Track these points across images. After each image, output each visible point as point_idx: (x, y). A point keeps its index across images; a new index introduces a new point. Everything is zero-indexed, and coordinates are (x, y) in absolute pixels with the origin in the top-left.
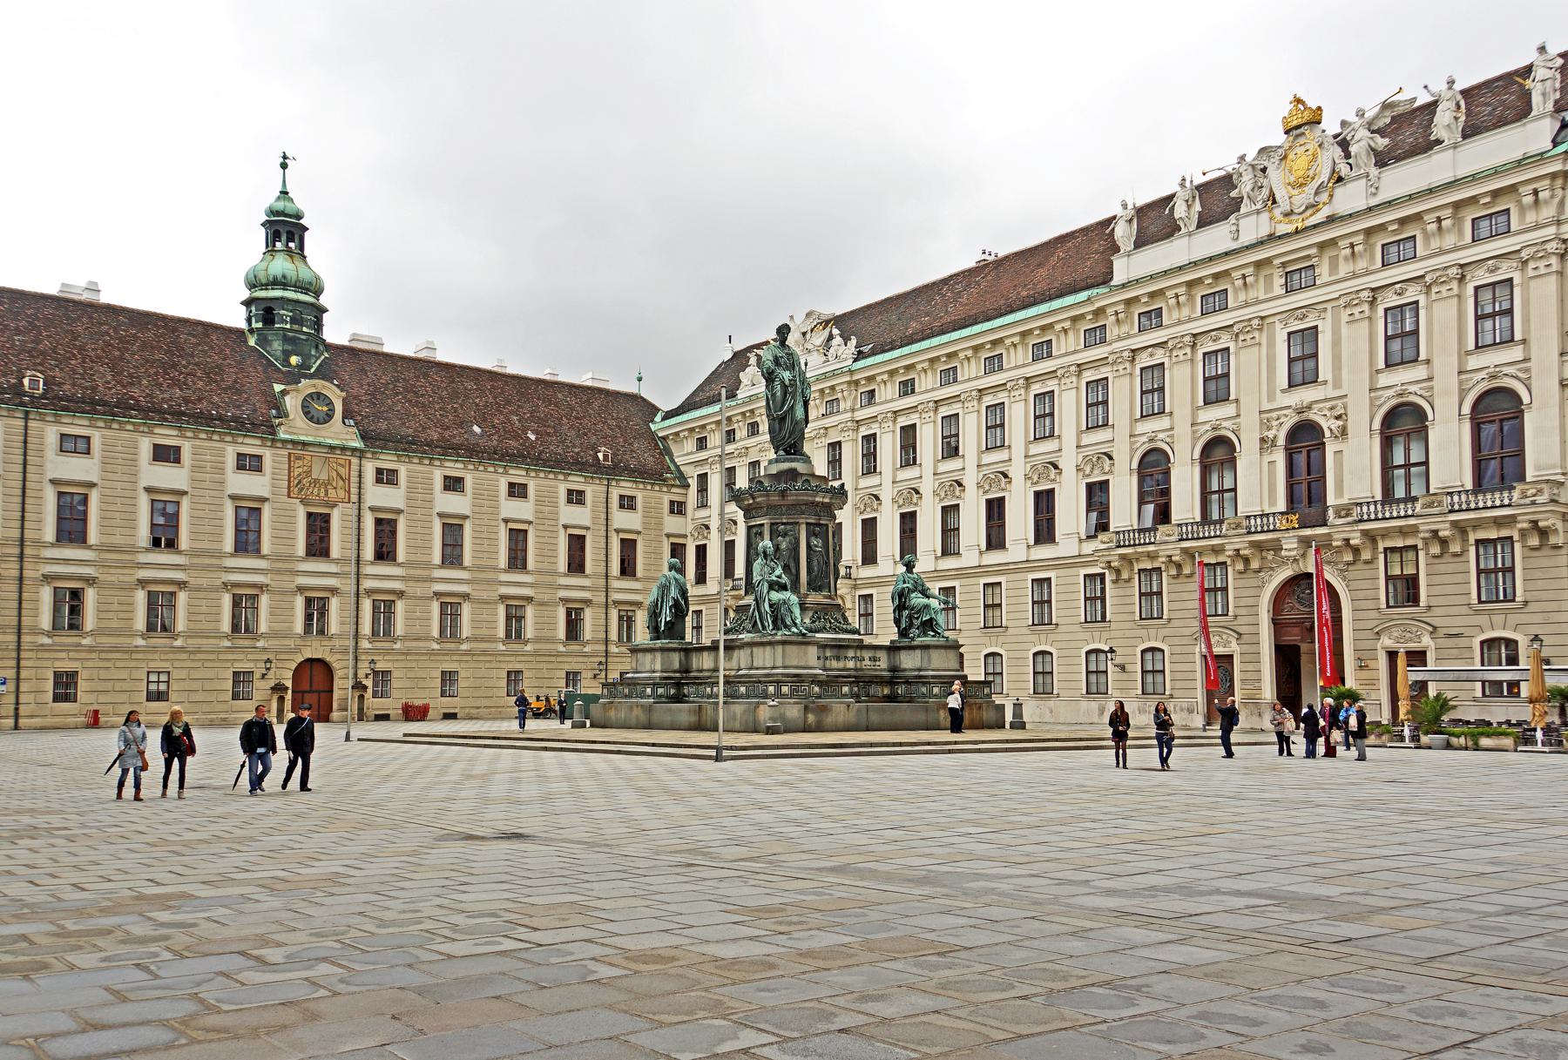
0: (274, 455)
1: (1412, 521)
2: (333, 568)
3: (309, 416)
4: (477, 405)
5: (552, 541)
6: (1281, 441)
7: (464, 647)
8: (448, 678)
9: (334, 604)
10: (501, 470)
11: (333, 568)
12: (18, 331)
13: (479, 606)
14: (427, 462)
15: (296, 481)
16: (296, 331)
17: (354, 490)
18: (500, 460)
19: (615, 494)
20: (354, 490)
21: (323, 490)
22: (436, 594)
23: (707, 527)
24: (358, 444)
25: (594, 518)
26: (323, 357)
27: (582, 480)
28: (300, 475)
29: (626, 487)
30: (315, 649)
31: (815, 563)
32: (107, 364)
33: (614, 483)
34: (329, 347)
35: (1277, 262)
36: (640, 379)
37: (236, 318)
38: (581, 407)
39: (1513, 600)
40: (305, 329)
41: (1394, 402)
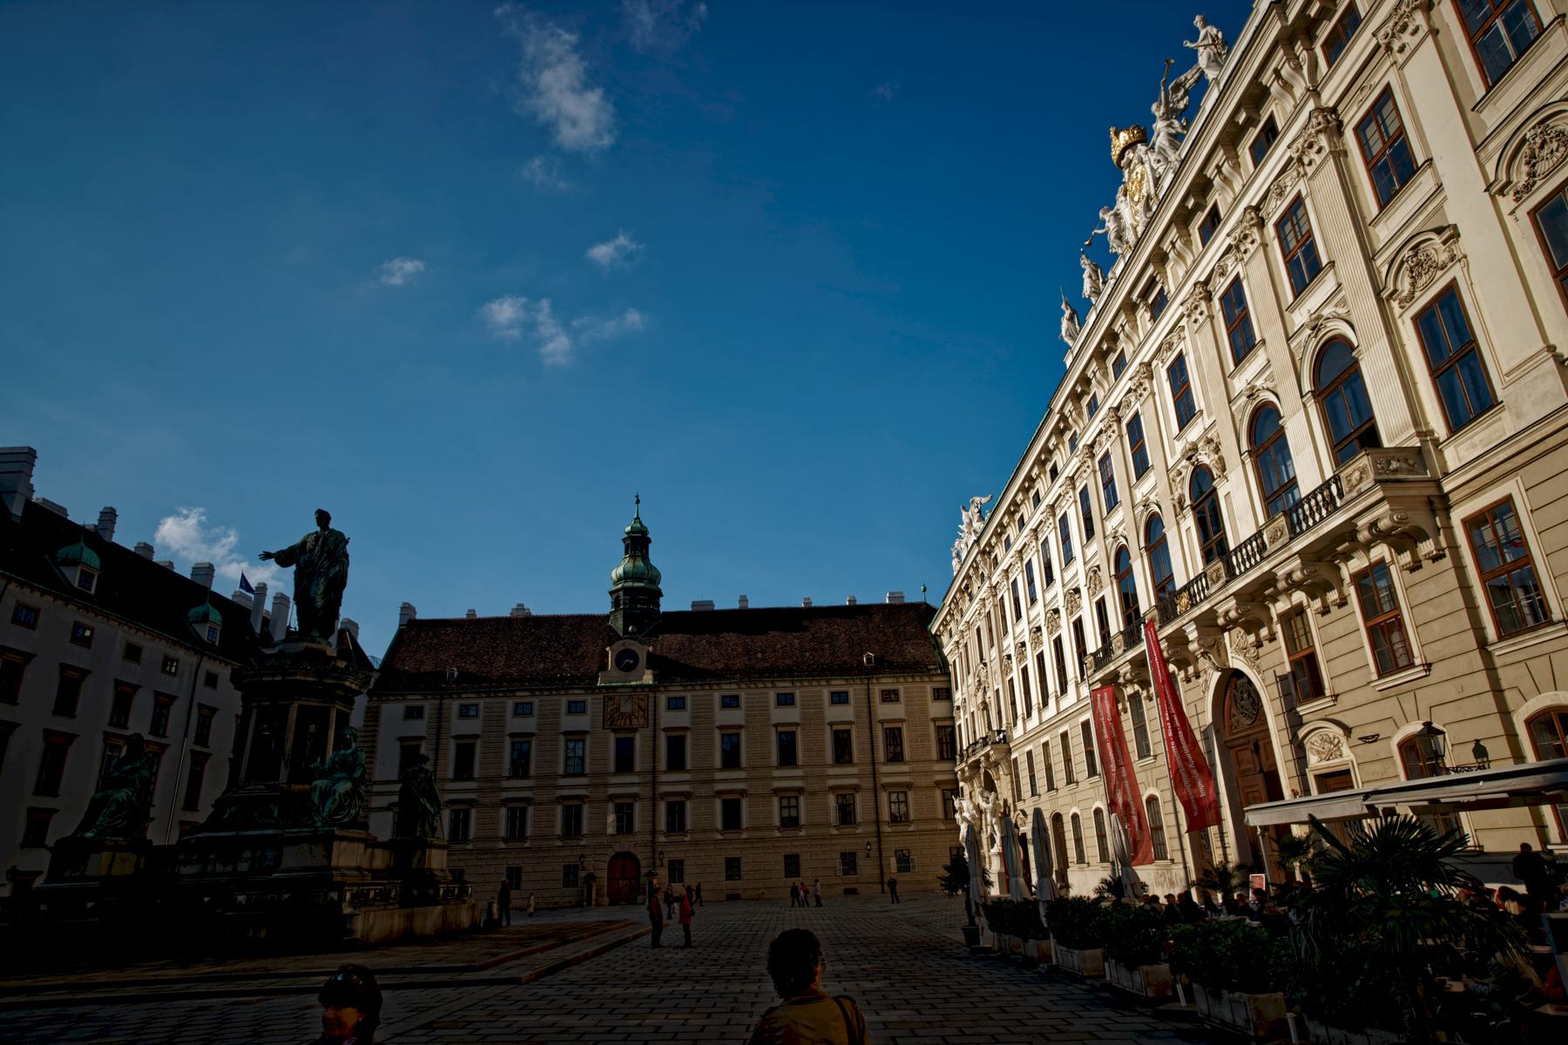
1: (1266, 567)
2: (636, 779)
6: (1188, 502)
7: (744, 836)
8: (733, 867)
9: (637, 806)
11: (636, 779)
17: (651, 717)
18: (769, 677)
19: (876, 691)
20: (651, 717)
30: (625, 844)
33: (874, 681)
35: (1134, 296)
36: (925, 590)
37: (603, 606)
39: (1411, 665)
41: (1250, 409)
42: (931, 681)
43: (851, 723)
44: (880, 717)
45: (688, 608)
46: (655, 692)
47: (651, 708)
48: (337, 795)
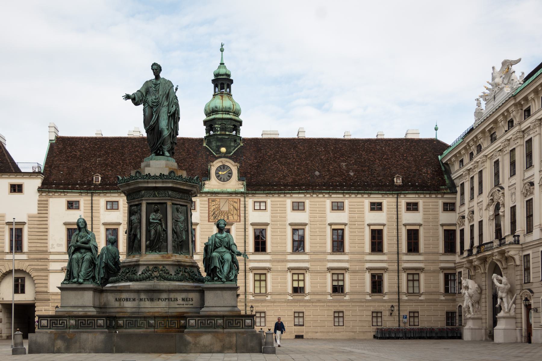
0: (200, 201)
3: (220, 178)
4: (321, 159)
5: (361, 234)
10: (327, 196)
12: (100, 156)
13: (314, 274)
14: (282, 195)
15: (212, 213)
16: (223, 135)
17: (242, 215)
19: (403, 202)
20: (242, 215)
21: (226, 216)
22: (289, 269)
23: (463, 217)
24: (242, 190)
25: (389, 219)
26: (239, 146)
27: (380, 196)
28: (214, 209)
29: (412, 198)
31: (153, 232)
32: (133, 166)
33: (402, 196)
34: (244, 140)
38: (391, 152)
40: (227, 133)
42: (442, 197)
43: (384, 225)
44: (404, 222)
45: (259, 136)
46: (245, 197)
47: (242, 209)
48: (230, 262)
